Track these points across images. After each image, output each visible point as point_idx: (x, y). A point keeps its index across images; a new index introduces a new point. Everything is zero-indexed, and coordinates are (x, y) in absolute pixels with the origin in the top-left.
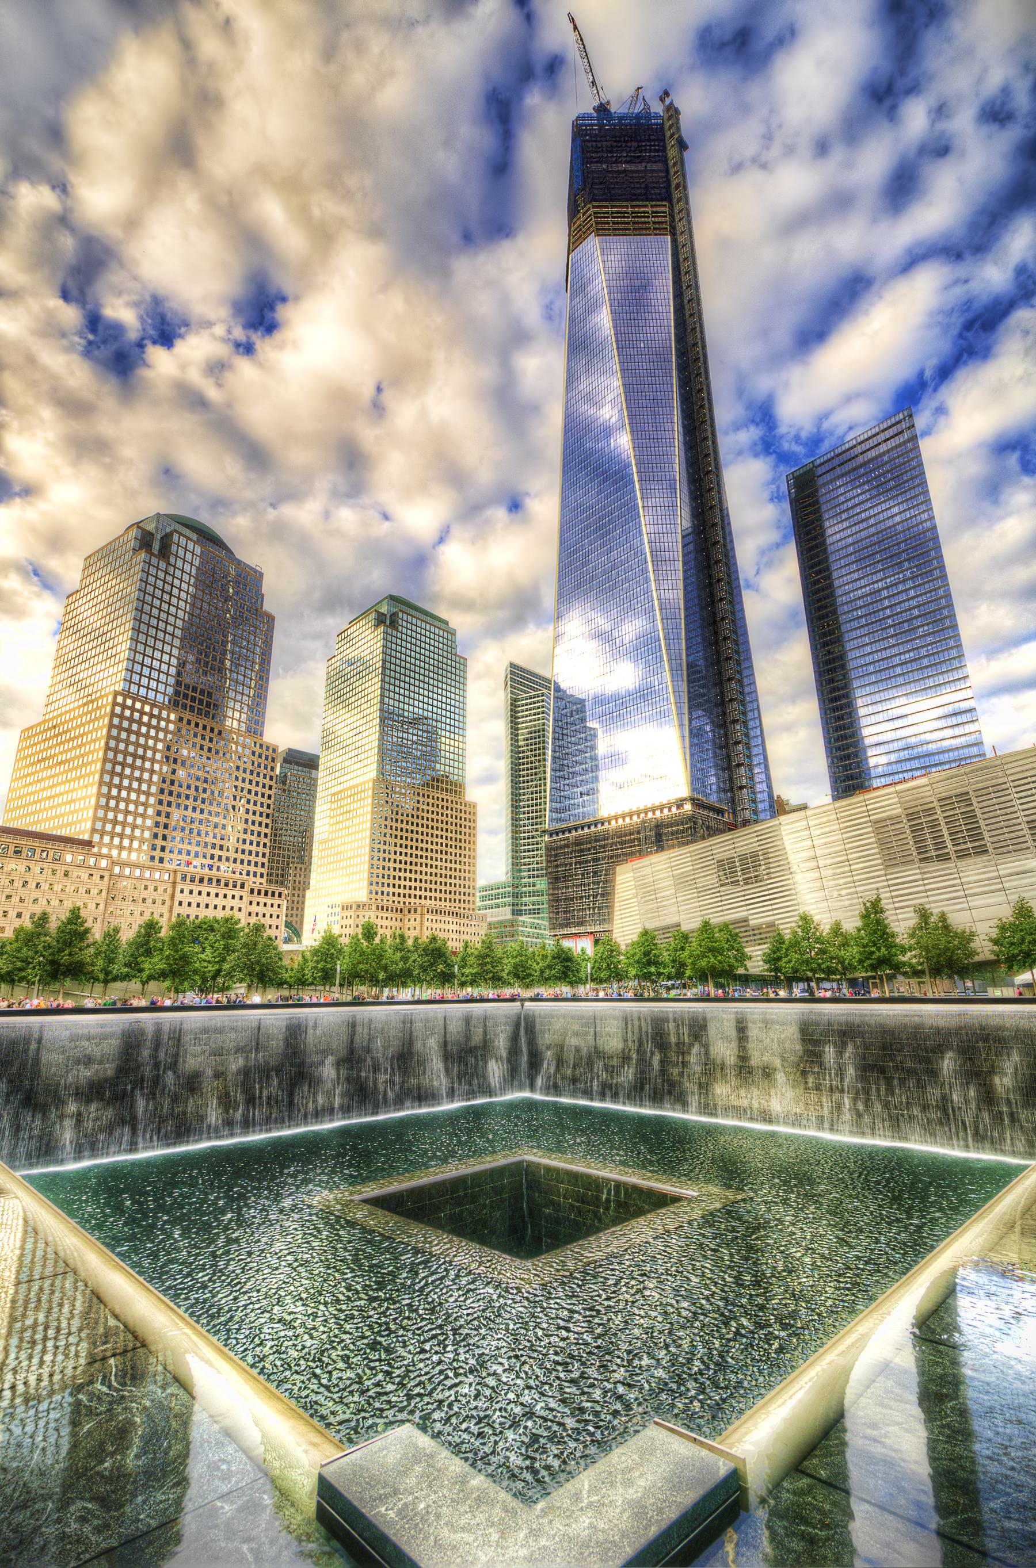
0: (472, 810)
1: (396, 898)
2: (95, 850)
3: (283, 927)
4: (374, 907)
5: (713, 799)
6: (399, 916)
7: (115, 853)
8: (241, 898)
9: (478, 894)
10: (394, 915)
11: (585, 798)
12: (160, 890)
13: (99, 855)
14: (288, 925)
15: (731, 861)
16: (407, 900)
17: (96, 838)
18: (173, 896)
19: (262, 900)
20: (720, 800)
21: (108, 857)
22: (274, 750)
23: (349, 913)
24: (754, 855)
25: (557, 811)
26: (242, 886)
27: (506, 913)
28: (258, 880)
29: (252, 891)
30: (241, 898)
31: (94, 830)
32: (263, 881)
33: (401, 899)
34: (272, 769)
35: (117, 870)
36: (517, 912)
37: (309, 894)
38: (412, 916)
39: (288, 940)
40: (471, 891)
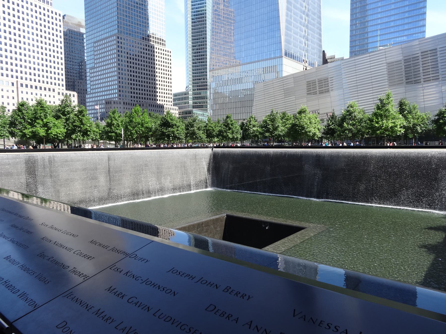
1: (133, 99)
4: (122, 103)
23: (109, 106)
26: (54, 90)
28: (61, 87)
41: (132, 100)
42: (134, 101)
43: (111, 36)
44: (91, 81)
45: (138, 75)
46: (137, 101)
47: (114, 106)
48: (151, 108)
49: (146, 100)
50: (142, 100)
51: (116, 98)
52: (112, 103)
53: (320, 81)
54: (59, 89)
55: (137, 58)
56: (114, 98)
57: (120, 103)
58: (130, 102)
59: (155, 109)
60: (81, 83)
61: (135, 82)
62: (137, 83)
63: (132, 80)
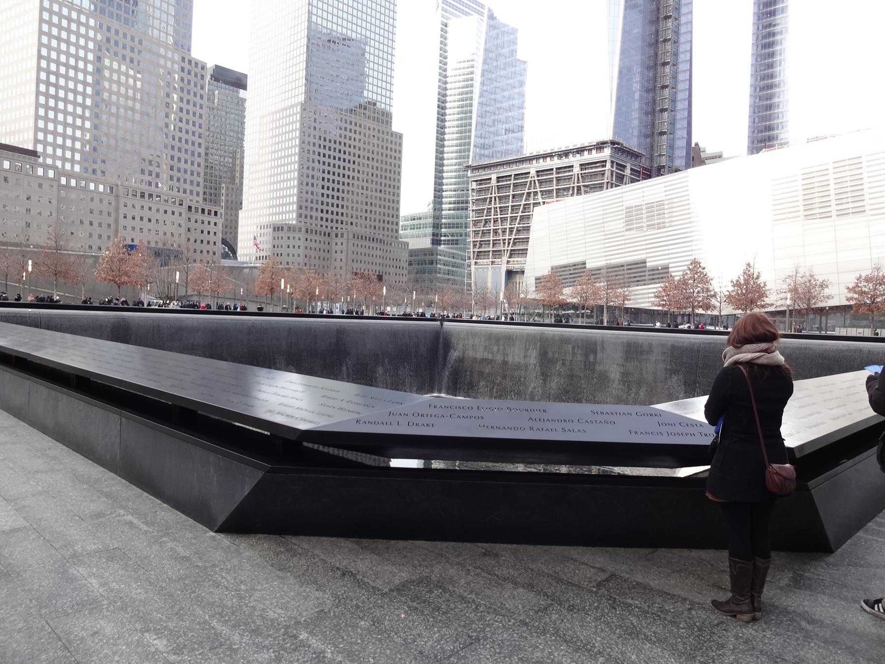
0: (398, 141)
1: (324, 223)
2: (41, 160)
3: (219, 243)
4: (303, 230)
5: (633, 144)
6: (327, 239)
7: (59, 164)
8: (180, 214)
9: (401, 223)
10: (322, 238)
11: (511, 135)
12: (105, 202)
13: (46, 167)
14: (224, 242)
15: (638, 207)
16: (334, 225)
17: (40, 148)
18: (117, 209)
19: (200, 217)
20: (640, 145)
21: (54, 167)
22: (203, 68)
23: (280, 234)
24: (660, 204)
25: (483, 147)
27: (426, 243)
28: (195, 198)
29: (190, 208)
30: (180, 214)
31: (36, 141)
32: (200, 199)
33: (329, 224)
34: (202, 88)
35: (63, 181)
36: (436, 242)
37: (241, 214)
38: (339, 240)
39: (225, 256)
40: (395, 220)
41: (322, 226)
42: (327, 227)
43: (292, 106)
44: (252, 188)
45: (336, 178)
46: (332, 228)
47: (289, 235)
48: (356, 242)
49: (349, 227)
50: (342, 226)
51: (292, 219)
52: (285, 229)
53: (650, 206)
54: (191, 200)
55: (337, 146)
56: (289, 219)
57: (300, 230)
58: (319, 228)
59: (364, 244)
60: (232, 189)
61: (330, 192)
62: (333, 193)
63: (326, 187)
